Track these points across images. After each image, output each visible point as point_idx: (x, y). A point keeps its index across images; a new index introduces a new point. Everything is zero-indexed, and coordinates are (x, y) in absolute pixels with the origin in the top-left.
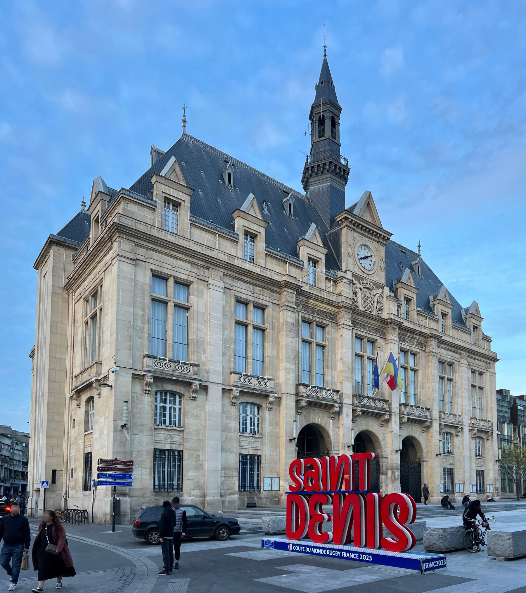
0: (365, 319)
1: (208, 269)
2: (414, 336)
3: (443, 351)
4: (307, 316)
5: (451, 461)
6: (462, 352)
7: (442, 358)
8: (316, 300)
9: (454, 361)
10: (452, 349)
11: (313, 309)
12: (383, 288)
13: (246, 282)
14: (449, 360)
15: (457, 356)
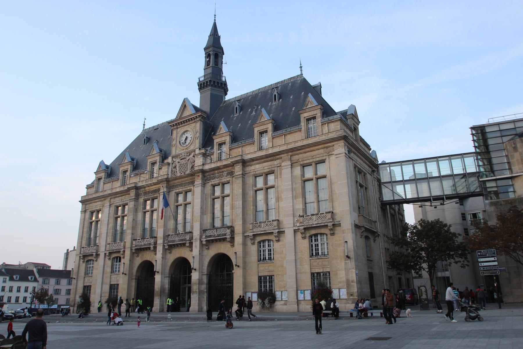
0: (180, 180)
1: (105, 200)
2: (222, 170)
3: (257, 166)
4: (146, 198)
5: (271, 268)
6: (282, 156)
7: (257, 172)
8: (149, 186)
9: (273, 169)
10: (268, 159)
11: (149, 192)
12: (195, 151)
13: (118, 197)
14: (265, 171)
15: (276, 162)
